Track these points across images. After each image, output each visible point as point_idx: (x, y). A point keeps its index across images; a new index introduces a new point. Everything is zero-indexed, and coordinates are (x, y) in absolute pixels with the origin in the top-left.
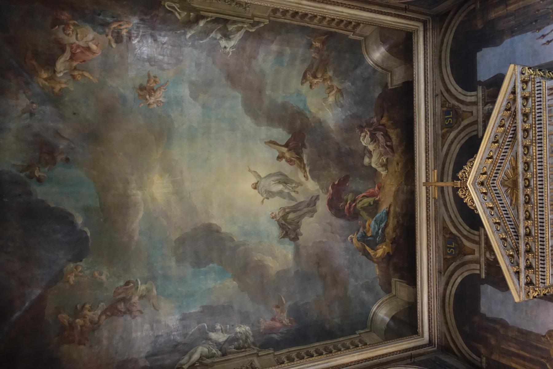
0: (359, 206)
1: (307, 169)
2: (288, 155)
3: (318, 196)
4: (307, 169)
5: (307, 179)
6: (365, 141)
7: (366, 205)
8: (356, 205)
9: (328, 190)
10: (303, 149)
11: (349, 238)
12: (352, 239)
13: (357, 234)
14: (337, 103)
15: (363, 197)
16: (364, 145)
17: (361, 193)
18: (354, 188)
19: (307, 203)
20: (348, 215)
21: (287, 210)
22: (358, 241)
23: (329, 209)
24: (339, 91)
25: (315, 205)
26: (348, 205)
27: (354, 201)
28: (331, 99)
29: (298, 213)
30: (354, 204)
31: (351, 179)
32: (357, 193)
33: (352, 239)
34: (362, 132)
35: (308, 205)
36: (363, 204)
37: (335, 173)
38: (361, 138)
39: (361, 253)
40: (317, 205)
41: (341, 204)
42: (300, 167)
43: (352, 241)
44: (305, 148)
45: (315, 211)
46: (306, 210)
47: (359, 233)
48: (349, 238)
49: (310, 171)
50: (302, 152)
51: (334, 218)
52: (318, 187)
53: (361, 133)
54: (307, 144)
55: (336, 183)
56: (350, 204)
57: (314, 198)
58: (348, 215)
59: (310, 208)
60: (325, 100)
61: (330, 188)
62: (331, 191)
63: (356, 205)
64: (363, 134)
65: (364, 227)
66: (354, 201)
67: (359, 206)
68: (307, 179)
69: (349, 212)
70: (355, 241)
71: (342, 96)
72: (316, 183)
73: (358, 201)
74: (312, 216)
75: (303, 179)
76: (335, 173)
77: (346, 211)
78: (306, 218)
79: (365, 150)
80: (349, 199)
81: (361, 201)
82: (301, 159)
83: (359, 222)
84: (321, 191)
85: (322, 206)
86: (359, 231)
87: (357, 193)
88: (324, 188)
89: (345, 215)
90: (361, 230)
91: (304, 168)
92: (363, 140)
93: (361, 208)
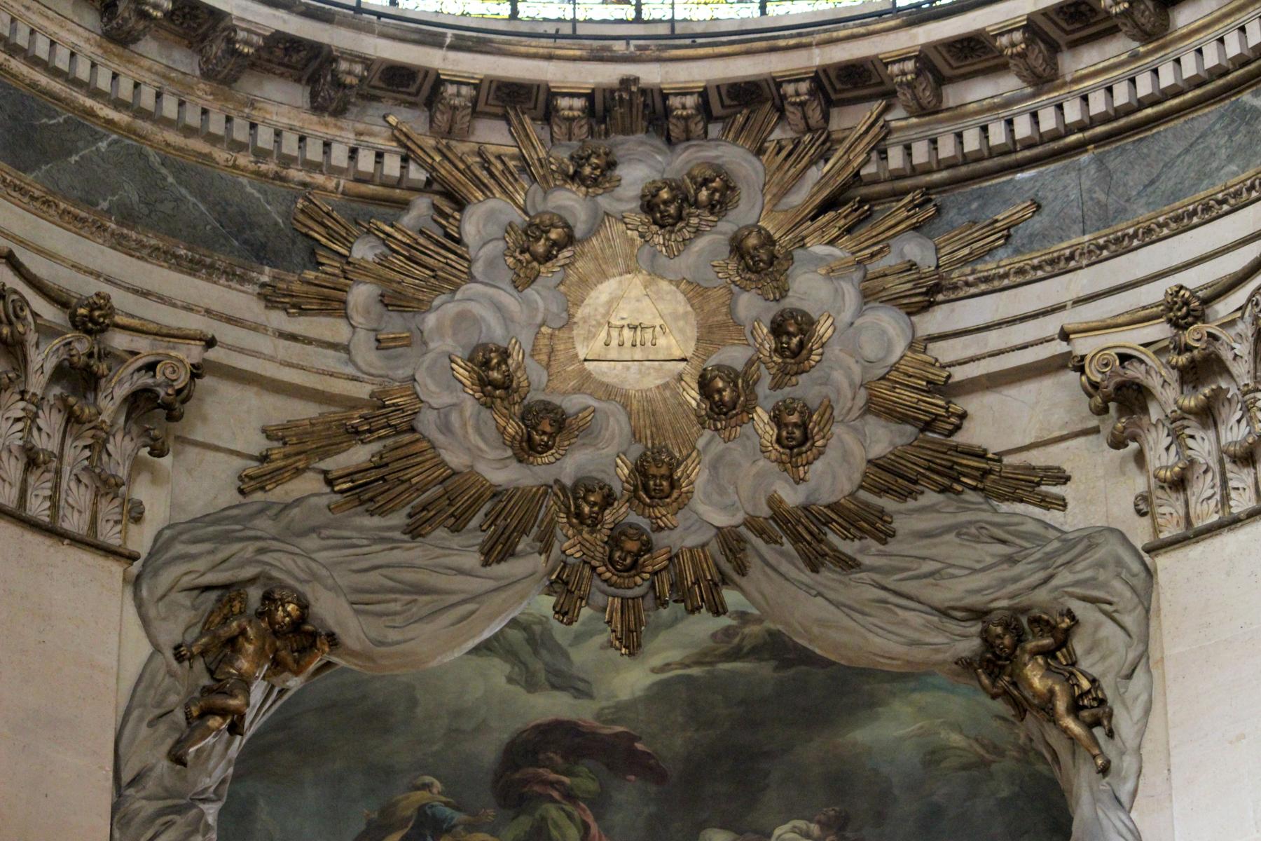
0: (553, 812)
1: (695, 671)
2: (753, 629)
3: (589, 696)
4: (695, 671)
5: (654, 670)
6: (792, 835)
7: (554, 833)
8: (552, 800)
9: (614, 722)
10: (773, 663)
11: (428, 779)
12: (427, 787)
13: (447, 804)
14: (934, 756)
15: (586, 827)
16: (777, 832)
17: (598, 818)
18: (619, 797)
19: (564, 668)
20: (517, 776)
21: (537, 628)
22: (421, 809)
23: (538, 726)
24: (983, 764)
25: (554, 687)
26: (553, 776)
27: (570, 796)
28: (956, 739)
29: (525, 652)
30: (556, 795)
31: (653, 789)
32: (599, 804)
33: (427, 787)
34: (824, 825)
35: (558, 673)
36: (557, 826)
37: (672, 743)
38: (801, 824)
39: (375, 816)
40: (558, 693)
41: (558, 759)
42: (705, 654)
43: (418, 788)
44: (776, 669)
45: (531, 686)
46: (537, 666)
47: (448, 811)
48: (428, 779)
49: (689, 677)
50: (760, 660)
51: (506, 737)
52: (624, 696)
53: (819, 822)
54: (791, 672)
55: (639, 746)
56: (562, 783)
57: (581, 685)
58: (517, 776)
59: (542, 676)
60: (957, 727)
61: (619, 729)
62: (607, 731)
63: (552, 800)
64: (815, 829)
65: (471, 828)
66: (570, 796)
67: (553, 812)
68: (654, 670)
69: (526, 782)
70: (420, 796)
71: (965, 767)
72: (639, 693)
73: (569, 808)
74: (510, 680)
75: (657, 661)
76: (672, 743)
77: (531, 770)
78: (507, 668)
79: (756, 832)
80: (578, 780)
81: (570, 816)
82: (736, 654)
83: (491, 812)
84: (611, 703)
85: (552, 706)
86: (457, 808)
87: (599, 804)
88: (620, 711)
89: (517, 768)
90: (459, 817)
91: (698, 663)
92: (794, 830)
93: (544, 819)
